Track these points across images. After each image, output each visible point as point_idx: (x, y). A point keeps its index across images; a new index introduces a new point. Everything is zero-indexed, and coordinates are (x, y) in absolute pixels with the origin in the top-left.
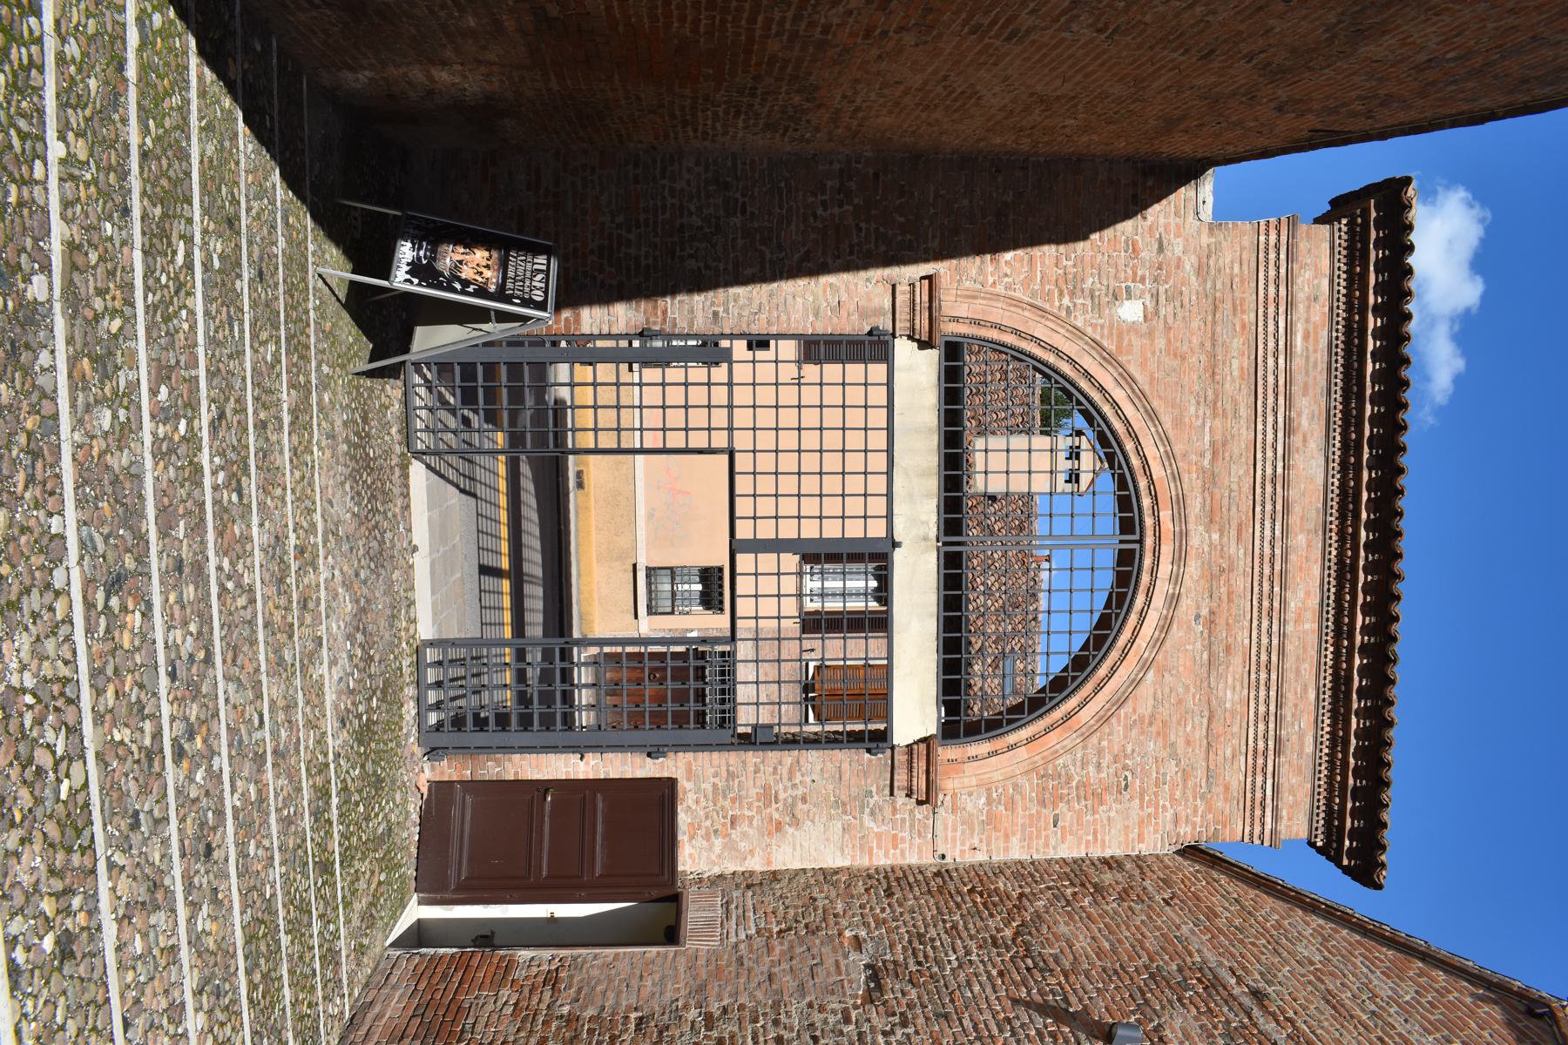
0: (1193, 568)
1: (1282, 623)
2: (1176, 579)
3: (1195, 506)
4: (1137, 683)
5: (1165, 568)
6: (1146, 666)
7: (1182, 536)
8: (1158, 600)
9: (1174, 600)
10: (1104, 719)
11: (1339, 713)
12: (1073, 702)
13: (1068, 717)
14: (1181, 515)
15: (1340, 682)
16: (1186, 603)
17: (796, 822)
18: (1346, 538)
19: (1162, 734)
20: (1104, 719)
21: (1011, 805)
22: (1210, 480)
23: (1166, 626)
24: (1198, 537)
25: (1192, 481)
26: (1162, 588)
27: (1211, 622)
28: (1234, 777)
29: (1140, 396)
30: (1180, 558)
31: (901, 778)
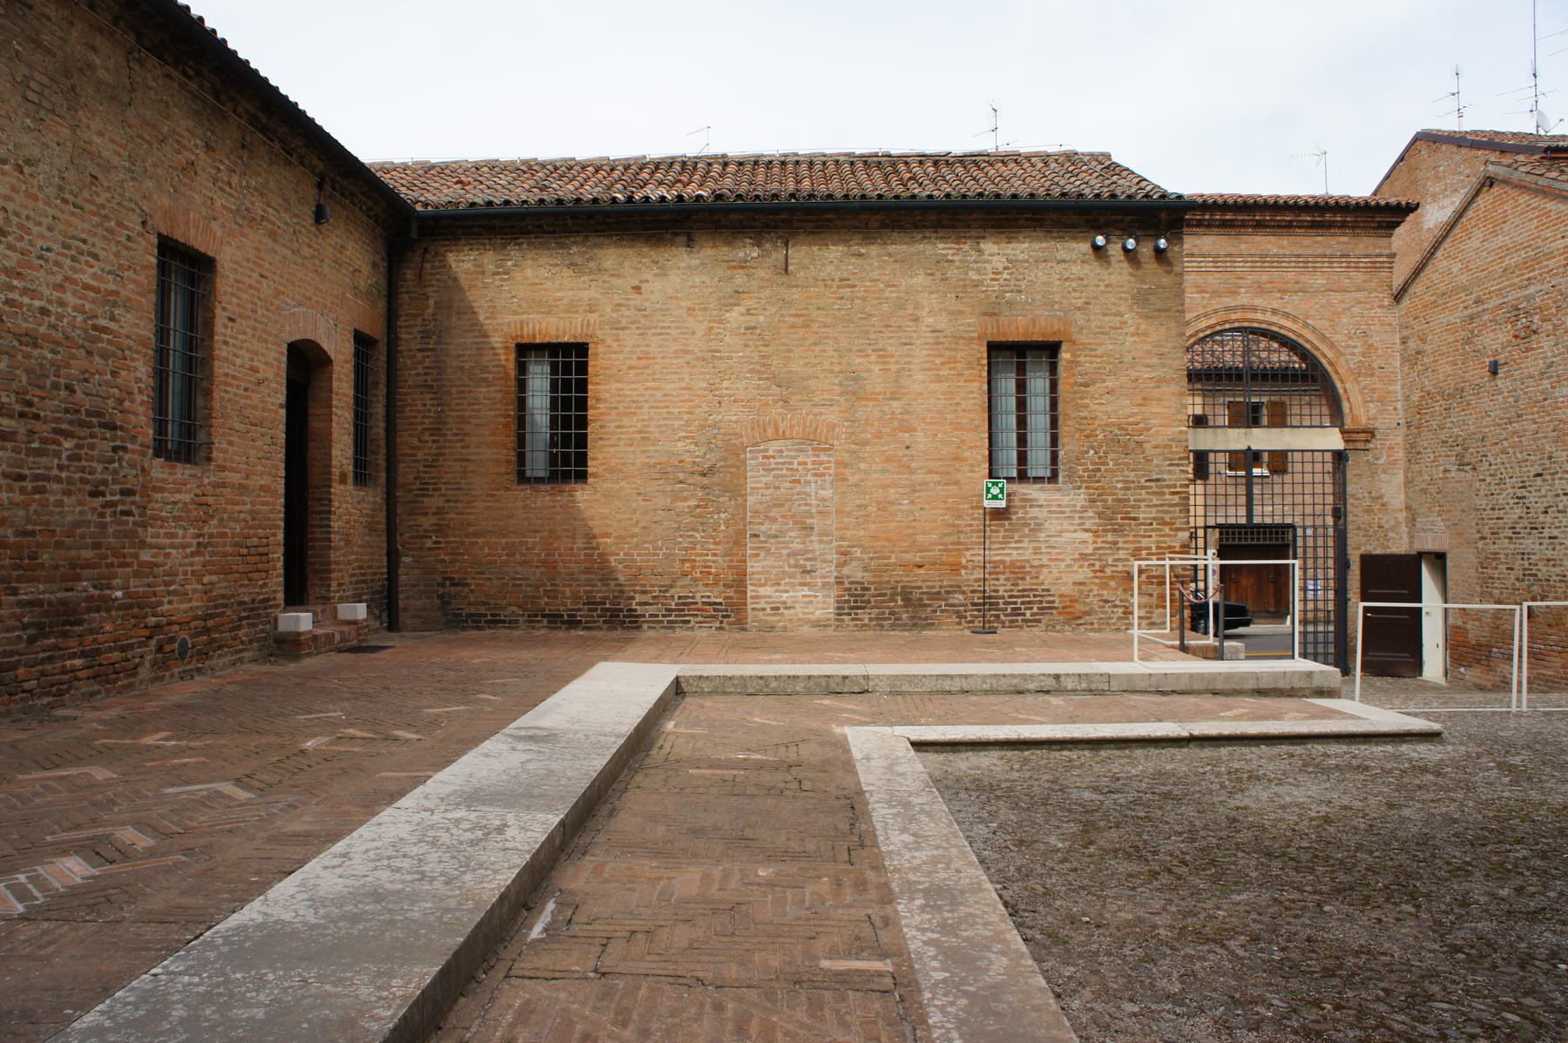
0: (1258, 302)
1: (1285, 256)
2: (1264, 311)
3: (1229, 301)
4: (1314, 330)
5: (1259, 316)
6: (1306, 325)
7: (1243, 308)
8: (1274, 319)
9: (1274, 312)
10: (1332, 345)
11: (1330, 225)
12: (1323, 361)
13: (1331, 363)
14: (1234, 309)
15: (1314, 225)
16: (1275, 305)
17: (1381, 497)
18: (1244, 225)
19: (1338, 315)
20: (1332, 345)
21: (1373, 390)
23: (1286, 315)
24: (1243, 299)
25: (1216, 303)
26: (1269, 317)
27: (1284, 291)
28: (1360, 277)
30: (1254, 309)
31: (1360, 445)
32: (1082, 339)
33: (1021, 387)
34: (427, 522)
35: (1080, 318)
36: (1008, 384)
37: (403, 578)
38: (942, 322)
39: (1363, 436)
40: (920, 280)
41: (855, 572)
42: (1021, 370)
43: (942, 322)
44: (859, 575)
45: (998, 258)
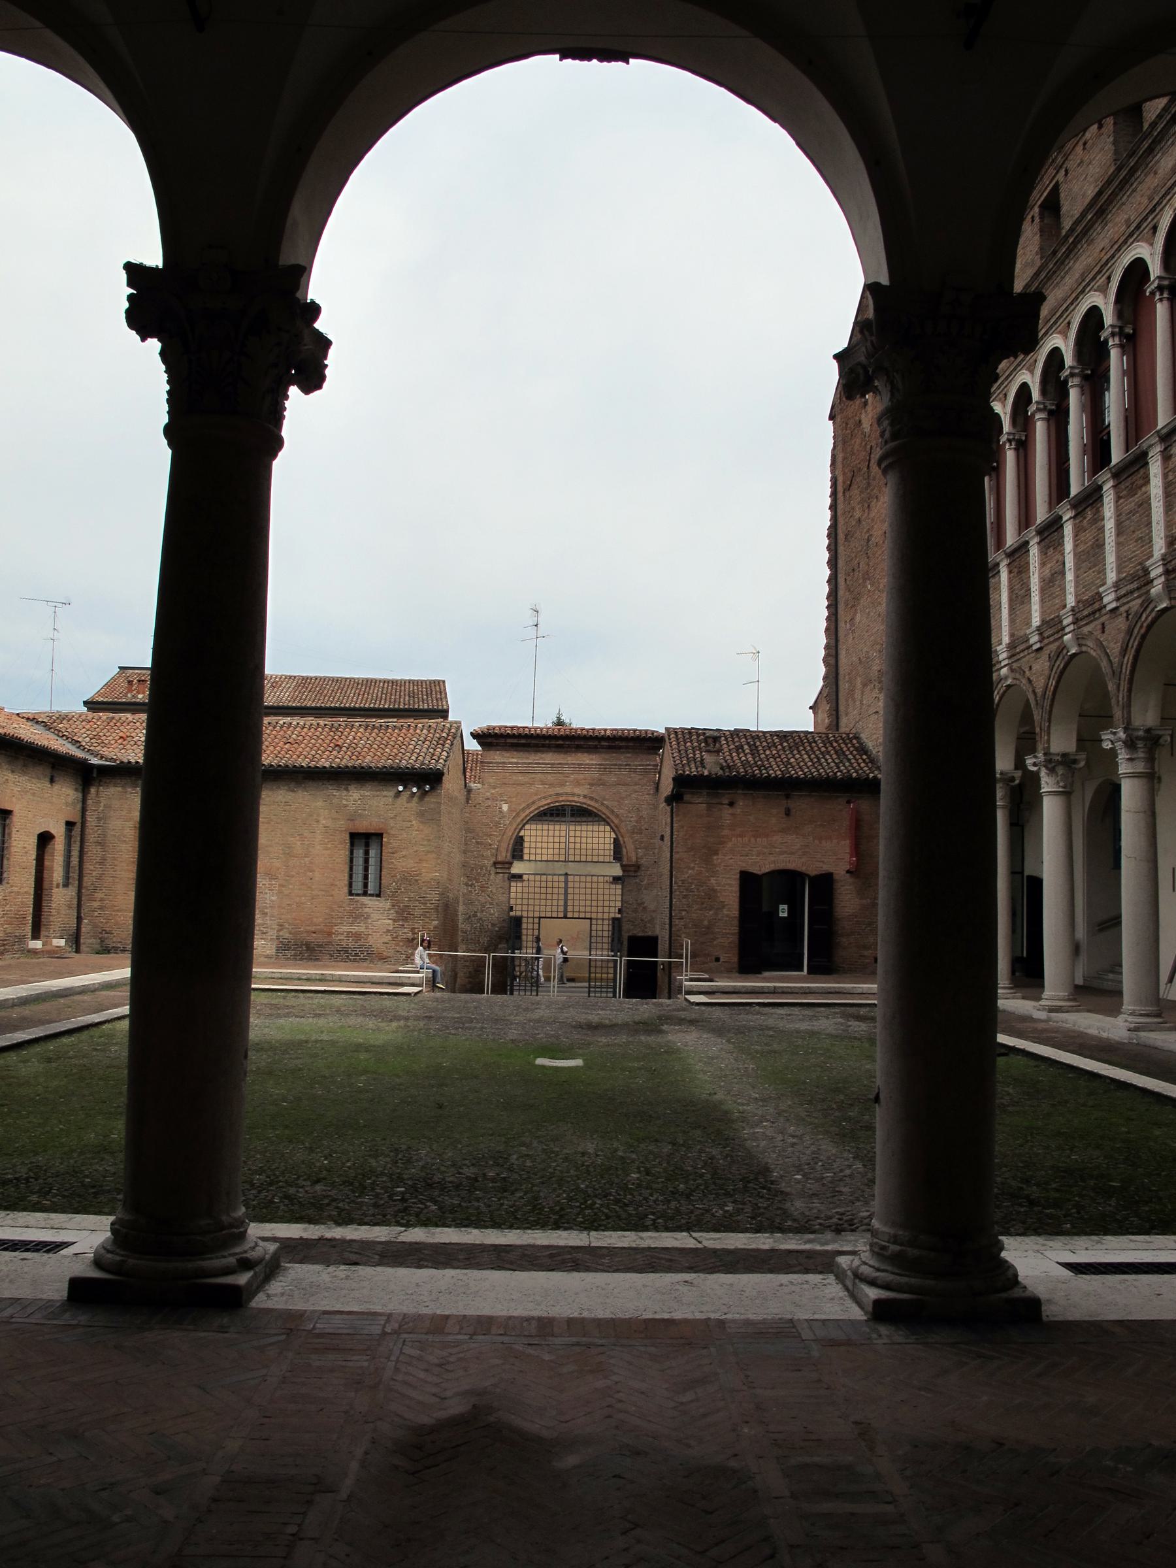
3: (559, 790)
4: (607, 807)
5: (576, 799)
10: (617, 816)
11: (620, 748)
14: (561, 794)
15: (609, 747)
18: (569, 746)
19: (623, 799)
20: (617, 816)
22: (552, 785)
24: (568, 789)
25: (553, 791)
29: (528, 806)
30: (573, 795)
31: (632, 874)
32: (392, 832)
33: (367, 853)
34: (96, 904)
35: (392, 823)
36: (359, 853)
37: (83, 930)
38: (329, 823)
39: (632, 869)
40: (320, 803)
41: (285, 934)
42: (367, 845)
43: (329, 823)
44: (287, 935)
45: (355, 797)
